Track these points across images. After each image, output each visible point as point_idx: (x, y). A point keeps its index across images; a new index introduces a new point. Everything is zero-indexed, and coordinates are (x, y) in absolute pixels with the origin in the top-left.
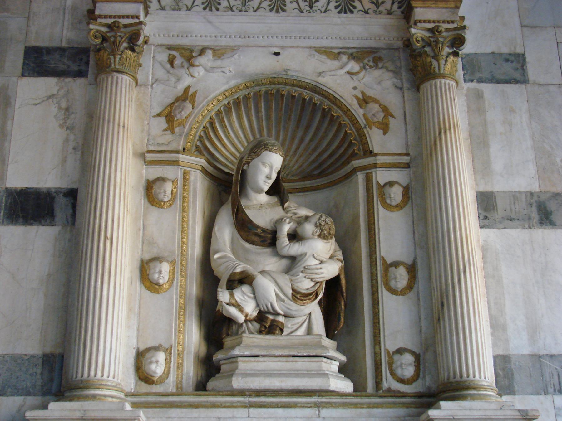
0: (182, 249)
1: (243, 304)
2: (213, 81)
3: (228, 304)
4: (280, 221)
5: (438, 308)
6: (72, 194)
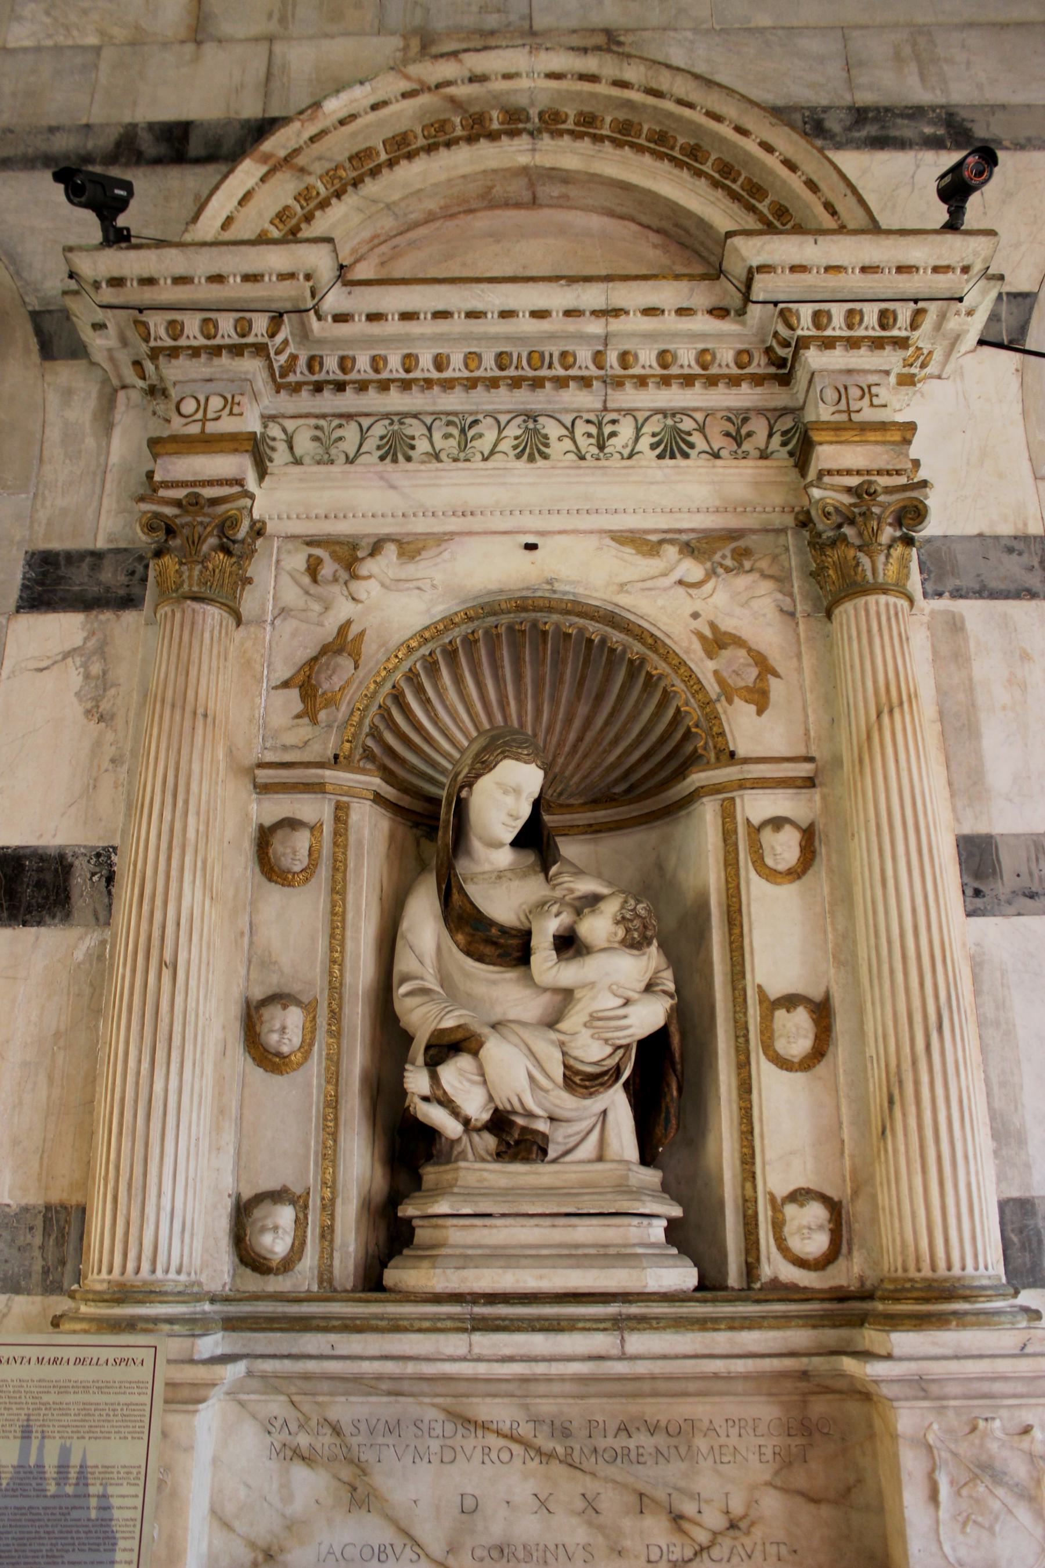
0: (331, 974)
1: (459, 1100)
2: (397, 607)
3: (426, 1099)
4: (541, 907)
5: (881, 1106)
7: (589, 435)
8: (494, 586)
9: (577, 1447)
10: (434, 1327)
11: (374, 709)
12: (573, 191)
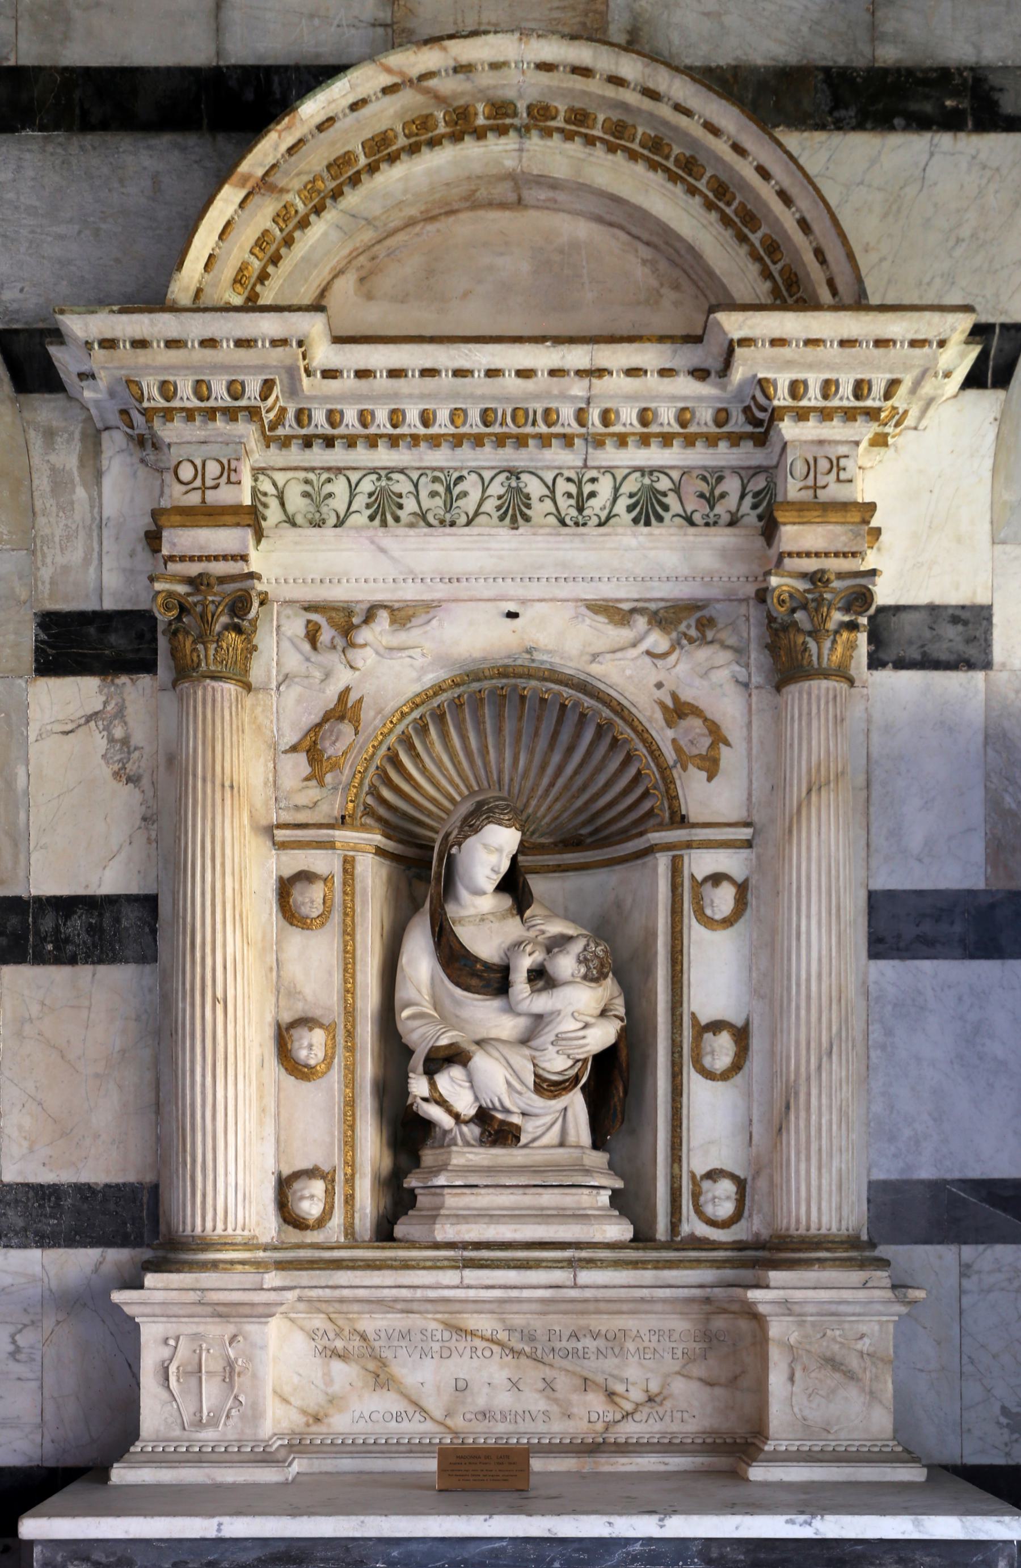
0: (346, 1001)
2: (393, 673)
7: (570, 495)
8: (477, 654)
9: (540, 1348)
10: (435, 1266)
11: (372, 770)
12: (561, 197)
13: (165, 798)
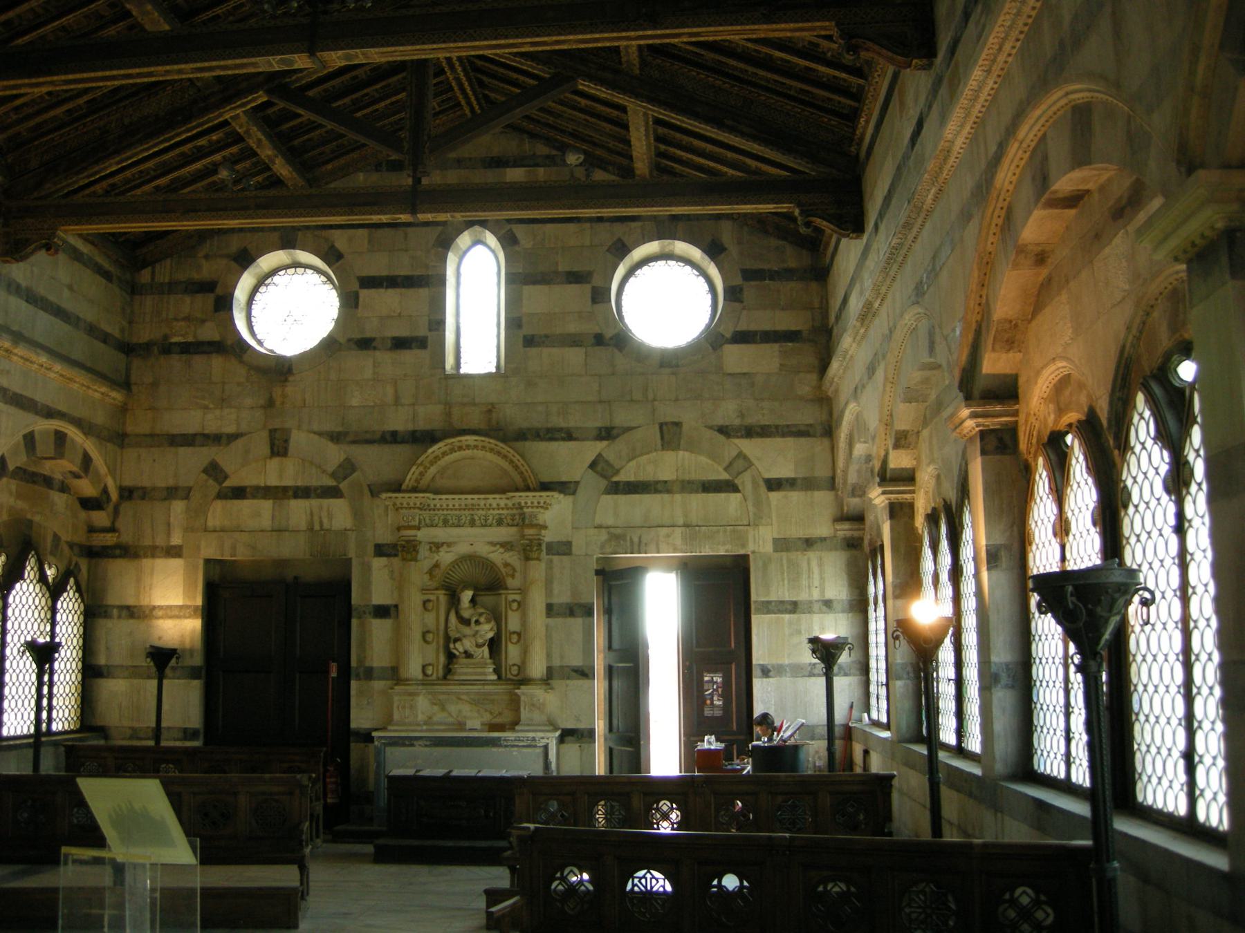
2: (446, 557)
6: (396, 606)
13: (400, 583)
